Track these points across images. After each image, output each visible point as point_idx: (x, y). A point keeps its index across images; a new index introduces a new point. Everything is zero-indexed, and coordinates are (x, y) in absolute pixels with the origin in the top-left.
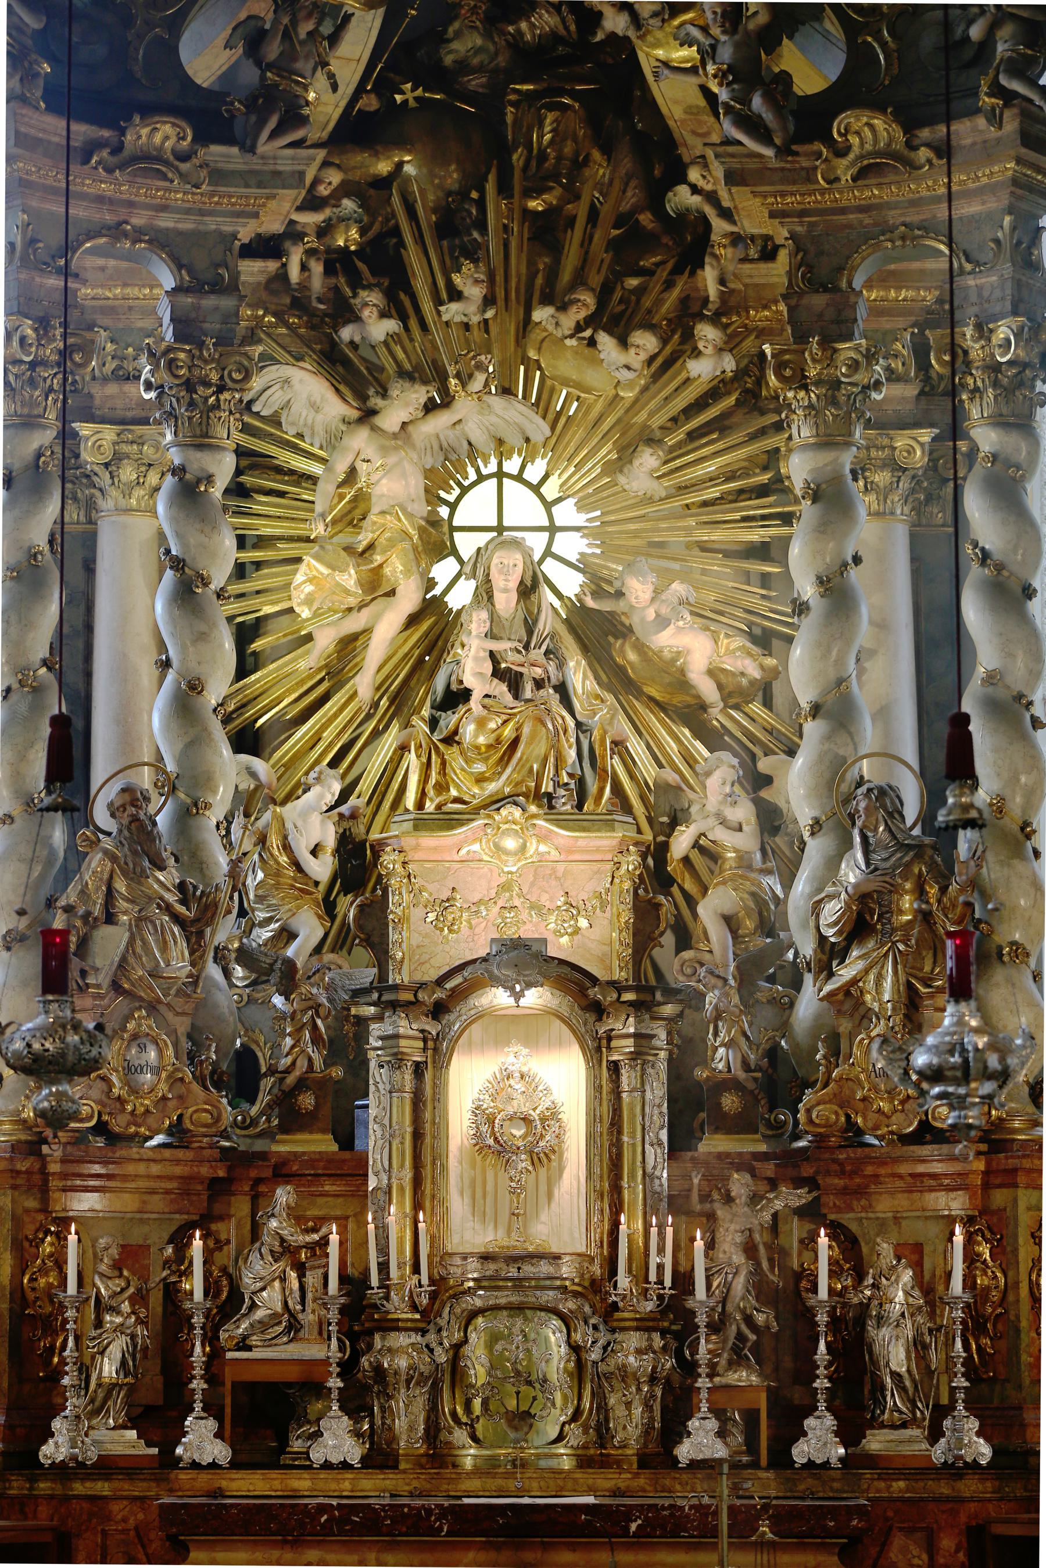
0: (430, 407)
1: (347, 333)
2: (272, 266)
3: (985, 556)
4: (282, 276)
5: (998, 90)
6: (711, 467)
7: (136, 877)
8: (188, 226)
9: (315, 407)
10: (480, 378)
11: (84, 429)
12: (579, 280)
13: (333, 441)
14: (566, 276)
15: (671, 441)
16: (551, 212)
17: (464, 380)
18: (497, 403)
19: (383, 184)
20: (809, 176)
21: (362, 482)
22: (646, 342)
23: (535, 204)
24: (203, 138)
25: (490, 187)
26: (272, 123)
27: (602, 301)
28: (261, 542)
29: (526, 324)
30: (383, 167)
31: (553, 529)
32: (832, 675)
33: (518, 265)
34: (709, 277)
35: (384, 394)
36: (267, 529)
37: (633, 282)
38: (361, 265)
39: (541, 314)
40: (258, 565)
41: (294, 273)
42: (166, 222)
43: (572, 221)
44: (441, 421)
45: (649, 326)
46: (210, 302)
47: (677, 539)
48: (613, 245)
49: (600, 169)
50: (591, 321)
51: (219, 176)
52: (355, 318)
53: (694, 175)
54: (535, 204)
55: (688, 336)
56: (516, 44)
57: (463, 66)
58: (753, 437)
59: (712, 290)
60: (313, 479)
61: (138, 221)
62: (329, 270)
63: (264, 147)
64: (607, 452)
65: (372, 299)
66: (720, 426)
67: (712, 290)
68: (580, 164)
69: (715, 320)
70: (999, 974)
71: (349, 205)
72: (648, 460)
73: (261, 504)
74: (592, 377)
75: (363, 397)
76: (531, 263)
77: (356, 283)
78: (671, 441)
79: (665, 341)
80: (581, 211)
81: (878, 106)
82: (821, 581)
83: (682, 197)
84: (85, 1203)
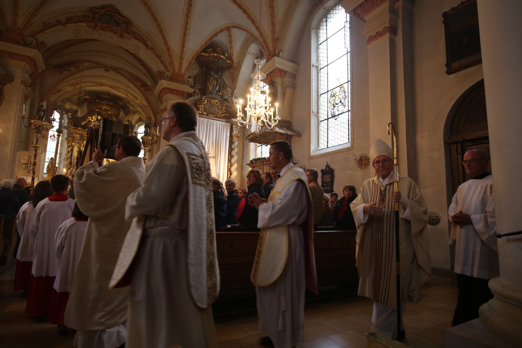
24: (82, 129)
42: (79, 133)
46: (82, 138)
51: (83, 131)
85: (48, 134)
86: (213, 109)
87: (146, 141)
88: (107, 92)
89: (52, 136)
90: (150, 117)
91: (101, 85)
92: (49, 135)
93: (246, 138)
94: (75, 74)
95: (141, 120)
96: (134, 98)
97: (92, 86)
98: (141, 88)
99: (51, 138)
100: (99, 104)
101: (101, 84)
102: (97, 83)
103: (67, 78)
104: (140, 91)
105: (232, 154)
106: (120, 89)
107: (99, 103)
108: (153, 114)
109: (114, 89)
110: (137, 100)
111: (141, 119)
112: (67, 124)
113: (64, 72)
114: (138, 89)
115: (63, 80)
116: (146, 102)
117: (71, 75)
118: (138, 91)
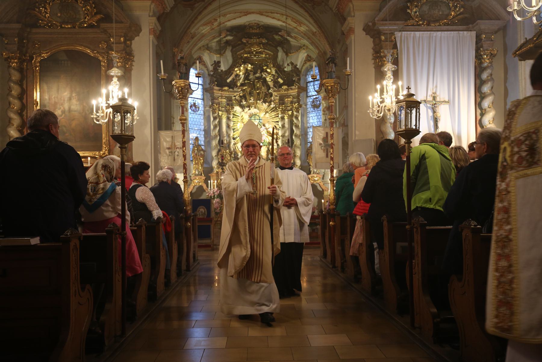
0: (249, 110)
1: (241, 103)
2: (235, 97)
3: (295, 123)
4: (236, 98)
5: (295, 84)
6: (273, 115)
7: (226, 151)
8: (228, 96)
9: (239, 110)
10: (253, 107)
11: (219, 112)
12: (261, 98)
13: (240, 113)
14: (260, 98)
15: (269, 112)
16: (259, 92)
17: (252, 107)
18: (254, 109)
19: (244, 90)
20: (280, 91)
21: (243, 117)
22: (267, 104)
23: (258, 91)
25: (254, 90)
26: (235, 87)
27: (263, 100)
28: (234, 122)
29: (257, 102)
30: (244, 88)
31: (260, 119)
32: (283, 133)
33: (256, 97)
34: (272, 98)
35: (245, 109)
36: (235, 120)
37: (266, 98)
38: (243, 97)
39: (258, 101)
40: (234, 123)
41: (237, 98)
42: (226, 95)
43: (261, 93)
44: (250, 111)
45: (267, 102)
46: (230, 102)
47: (270, 121)
48: (265, 95)
49: (263, 88)
50: (263, 102)
51: (231, 92)
52: (242, 102)
53: (271, 89)
54: (258, 91)
55: (271, 103)
56: (256, 77)
57: (251, 79)
58: (277, 112)
59: (273, 99)
60: (239, 116)
61: (224, 95)
62: (240, 98)
63: (235, 89)
64: (264, 113)
65: (243, 100)
66: (274, 111)
67: (273, 99)
68: (261, 88)
69: (273, 102)
70: (296, 158)
71: (241, 92)
72: (267, 114)
73: (234, 118)
74: (263, 107)
75: (243, 109)
76: (257, 97)
77: (242, 99)
78: (269, 112)
79: (269, 103)
80: (261, 92)
81: (286, 85)
82: (282, 125)
83: (270, 91)
84: (222, 177)
85: (187, 104)
86: (437, 10)
87: (329, 88)
88: (255, 23)
89: (193, 106)
90: (324, 52)
91: (246, 13)
92: (189, 105)
93: (515, 53)
94: (210, 4)
95: (310, 59)
96: (296, 25)
97: (235, 19)
98: (306, 4)
99: (192, 108)
100: (247, 45)
101: (247, 12)
102: (241, 12)
103: (200, 13)
104: (304, 9)
105: (483, 92)
106: (274, 13)
107: (247, 44)
108: (329, 44)
109: (265, 15)
110: (301, 27)
111: (310, 57)
112: (209, 84)
113: (196, 5)
114: (301, 7)
115: (196, 18)
116: (315, 25)
117: (205, 8)
118: (302, 11)
